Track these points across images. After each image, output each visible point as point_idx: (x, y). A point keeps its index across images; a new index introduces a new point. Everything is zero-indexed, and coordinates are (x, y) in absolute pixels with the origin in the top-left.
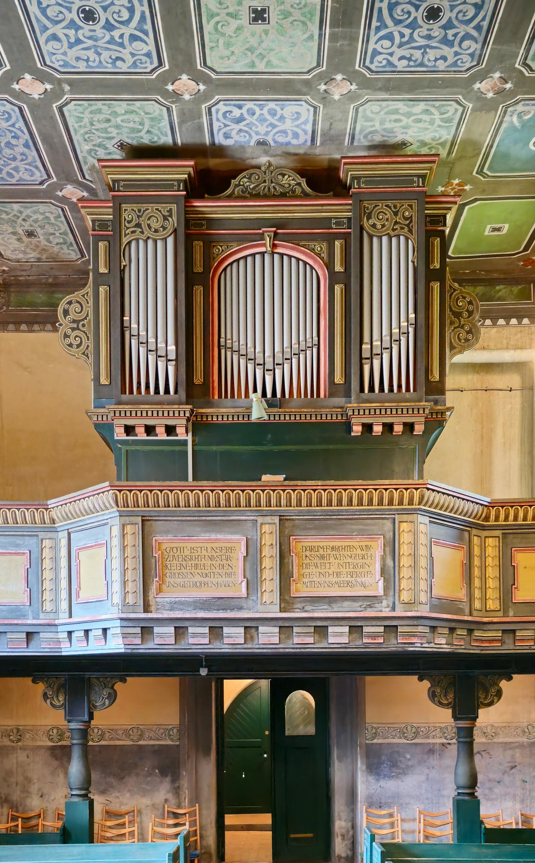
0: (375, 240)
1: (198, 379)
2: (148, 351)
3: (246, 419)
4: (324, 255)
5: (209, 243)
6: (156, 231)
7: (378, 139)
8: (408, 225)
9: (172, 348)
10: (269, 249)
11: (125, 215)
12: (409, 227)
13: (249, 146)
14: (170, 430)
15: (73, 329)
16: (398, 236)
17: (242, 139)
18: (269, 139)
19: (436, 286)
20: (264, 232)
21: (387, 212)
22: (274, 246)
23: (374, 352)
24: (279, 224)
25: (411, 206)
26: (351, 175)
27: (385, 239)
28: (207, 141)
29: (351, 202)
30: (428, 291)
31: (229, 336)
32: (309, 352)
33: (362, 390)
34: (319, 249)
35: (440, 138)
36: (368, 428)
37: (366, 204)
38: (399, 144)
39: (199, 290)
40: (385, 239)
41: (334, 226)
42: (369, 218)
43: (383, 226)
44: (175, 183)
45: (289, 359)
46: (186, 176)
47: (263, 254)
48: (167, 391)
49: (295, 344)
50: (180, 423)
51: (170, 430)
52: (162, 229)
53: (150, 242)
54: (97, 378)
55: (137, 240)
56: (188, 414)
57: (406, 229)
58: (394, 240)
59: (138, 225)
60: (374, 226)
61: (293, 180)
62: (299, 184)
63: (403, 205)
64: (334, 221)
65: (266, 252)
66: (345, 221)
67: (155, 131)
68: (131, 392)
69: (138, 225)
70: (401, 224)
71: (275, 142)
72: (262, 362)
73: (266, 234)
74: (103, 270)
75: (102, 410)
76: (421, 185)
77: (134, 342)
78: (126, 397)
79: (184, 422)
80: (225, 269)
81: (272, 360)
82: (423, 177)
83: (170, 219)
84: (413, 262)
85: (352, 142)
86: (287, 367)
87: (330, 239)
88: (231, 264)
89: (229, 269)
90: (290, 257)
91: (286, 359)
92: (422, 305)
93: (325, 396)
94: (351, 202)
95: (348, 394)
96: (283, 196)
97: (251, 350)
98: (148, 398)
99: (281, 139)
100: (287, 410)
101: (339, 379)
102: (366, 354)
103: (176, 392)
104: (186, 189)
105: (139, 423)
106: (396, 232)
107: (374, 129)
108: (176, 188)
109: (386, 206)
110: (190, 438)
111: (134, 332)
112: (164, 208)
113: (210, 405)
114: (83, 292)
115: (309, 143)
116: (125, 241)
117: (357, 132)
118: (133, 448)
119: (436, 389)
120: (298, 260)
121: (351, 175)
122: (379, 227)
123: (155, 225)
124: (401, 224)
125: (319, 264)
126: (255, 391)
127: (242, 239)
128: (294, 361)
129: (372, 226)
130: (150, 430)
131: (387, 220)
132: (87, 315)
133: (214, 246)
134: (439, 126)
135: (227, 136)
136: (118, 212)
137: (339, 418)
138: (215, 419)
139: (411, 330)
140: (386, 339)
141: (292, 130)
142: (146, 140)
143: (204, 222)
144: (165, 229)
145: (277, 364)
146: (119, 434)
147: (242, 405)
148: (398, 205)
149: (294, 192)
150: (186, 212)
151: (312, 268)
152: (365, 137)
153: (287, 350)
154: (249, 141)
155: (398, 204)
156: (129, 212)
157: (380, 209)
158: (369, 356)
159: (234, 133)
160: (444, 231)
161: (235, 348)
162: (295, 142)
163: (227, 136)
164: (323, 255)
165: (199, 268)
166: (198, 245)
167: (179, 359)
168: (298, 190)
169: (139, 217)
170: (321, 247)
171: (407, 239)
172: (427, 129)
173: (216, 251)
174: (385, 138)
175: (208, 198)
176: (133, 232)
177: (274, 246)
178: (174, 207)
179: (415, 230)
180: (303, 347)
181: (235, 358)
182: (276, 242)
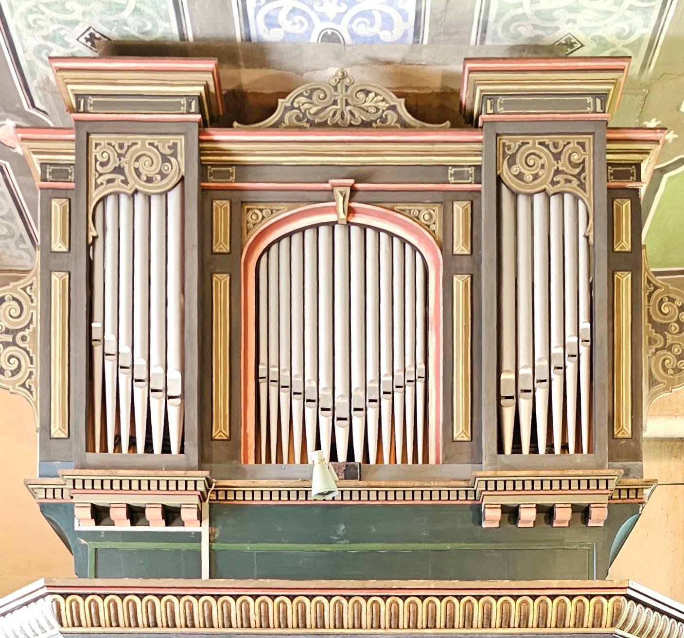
0: (522, 201)
1: (221, 431)
2: (134, 380)
3: (302, 497)
4: (437, 227)
5: (240, 204)
6: (149, 180)
7: (526, 33)
8: (577, 176)
9: (174, 375)
10: (343, 216)
11: (95, 152)
12: (579, 180)
13: (309, 43)
14: (171, 515)
15: (6, 345)
16: (561, 194)
17: (296, 30)
18: (343, 29)
19: (625, 279)
20: (334, 186)
21: (542, 155)
22: (351, 211)
23: (521, 386)
24: (361, 175)
25: (582, 145)
26: (482, 91)
27: (538, 200)
28: (239, 35)
30: (612, 285)
31: (273, 361)
32: (409, 389)
33: (501, 450)
34: (427, 217)
35: (631, 33)
36: (511, 513)
37: (505, 140)
38: (561, 44)
39: (221, 281)
40: (538, 200)
41: (452, 179)
42: (512, 162)
43: (536, 177)
44: (183, 101)
47: (332, 225)
48: (166, 449)
49: (386, 375)
50: (188, 504)
51: (171, 515)
52: (159, 177)
53: (139, 199)
54: (46, 427)
55: (117, 195)
56: (201, 487)
57: (575, 182)
58: (554, 201)
59: (119, 170)
60: (520, 176)
61: (383, 100)
62: (393, 108)
63: (569, 143)
64: (451, 171)
65: (336, 222)
66: (471, 171)
67: (149, 11)
68: (104, 449)
69: (119, 170)
70: (566, 174)
71: (353, 36)
72: (330, 406)
73: (337, 190)
74: (58, 245)
75: (54, 480)
76: (599, 109)
77: (110, 365)
78: (97, 456)
79: (196, 500)
80: (267, 250)
81: (347, 401)
82: (603, 96)
83: (173, 160)
84: (587, 238)
85: (483, 39)
86: (372, 413)
88: (278, 241)
89: (274, 248)
91: (371, 401)
92: (601, 309)
93: (437, 462)
95: (476, 458)
96: (366, 125)
97: (311, 384)
98: (132, 459)
99: (362, 30)
100: (373, 484)
101: (461, 432)
102: (507, 390)
103: (182, 451)
104: (201, 111)
105: (117, 503)
106: (557, 188)
108: (184, 109)
109: (540, 144)
110: (205, 530)
111: (110, 348)
112: (164, 142)
113: (240, 473)
114: (22, 283)
115: (410, 39)
116: (95, 195)
117: (491, 18)
118: (107, 545)
119: (628, 450)
120: (391, 235)
121: (482, 91)
122: (528, 177)
123: (147, 170)
124: (566, 174)
126: (318, 447)
127: (298, 198)
128: (386, 403)
129: (516, 176)
130: (135, 514)
131: (543, 166)
132: (31, 322)
133: (248, 210)
134: (631, 8)
135: (271, 22)
136: (85, 148)
137: (462, 496)
138: (248, 497)
139: (584, 350)
140: (542, 364)
142: (132, 28)
143: (232, 170)
144: (164, 176)
145: (356, 409)
146: (84, 522)
147: (297, 475)
148: (561, 144)
149: (384, 120)
150: (202, 152)
151: (415, 249)
152: (505, 28)
153: (372, 385)
154: (309, 33)
155: (561, 140)
156: (103, 147)
158: (513, 394)
159: (282, 17)
160: (636, 190)
162: (386, 36)
163: (271, 22)
164: (433, 227)
165: (222, 245)
166: (221, 208)
167: (187, 394)
168: (392, 118)
169: (120, 156)
170: (431, 213)
171: (576, 199)
172: (609, 13)
173: (251, 218)
174: (539, 32)
175: (237, 127)
176: (110, 181)
177: (351, 211)
178: (181, 141)
179: (589, 185)
181: (285, 395)
182: (354, 205)
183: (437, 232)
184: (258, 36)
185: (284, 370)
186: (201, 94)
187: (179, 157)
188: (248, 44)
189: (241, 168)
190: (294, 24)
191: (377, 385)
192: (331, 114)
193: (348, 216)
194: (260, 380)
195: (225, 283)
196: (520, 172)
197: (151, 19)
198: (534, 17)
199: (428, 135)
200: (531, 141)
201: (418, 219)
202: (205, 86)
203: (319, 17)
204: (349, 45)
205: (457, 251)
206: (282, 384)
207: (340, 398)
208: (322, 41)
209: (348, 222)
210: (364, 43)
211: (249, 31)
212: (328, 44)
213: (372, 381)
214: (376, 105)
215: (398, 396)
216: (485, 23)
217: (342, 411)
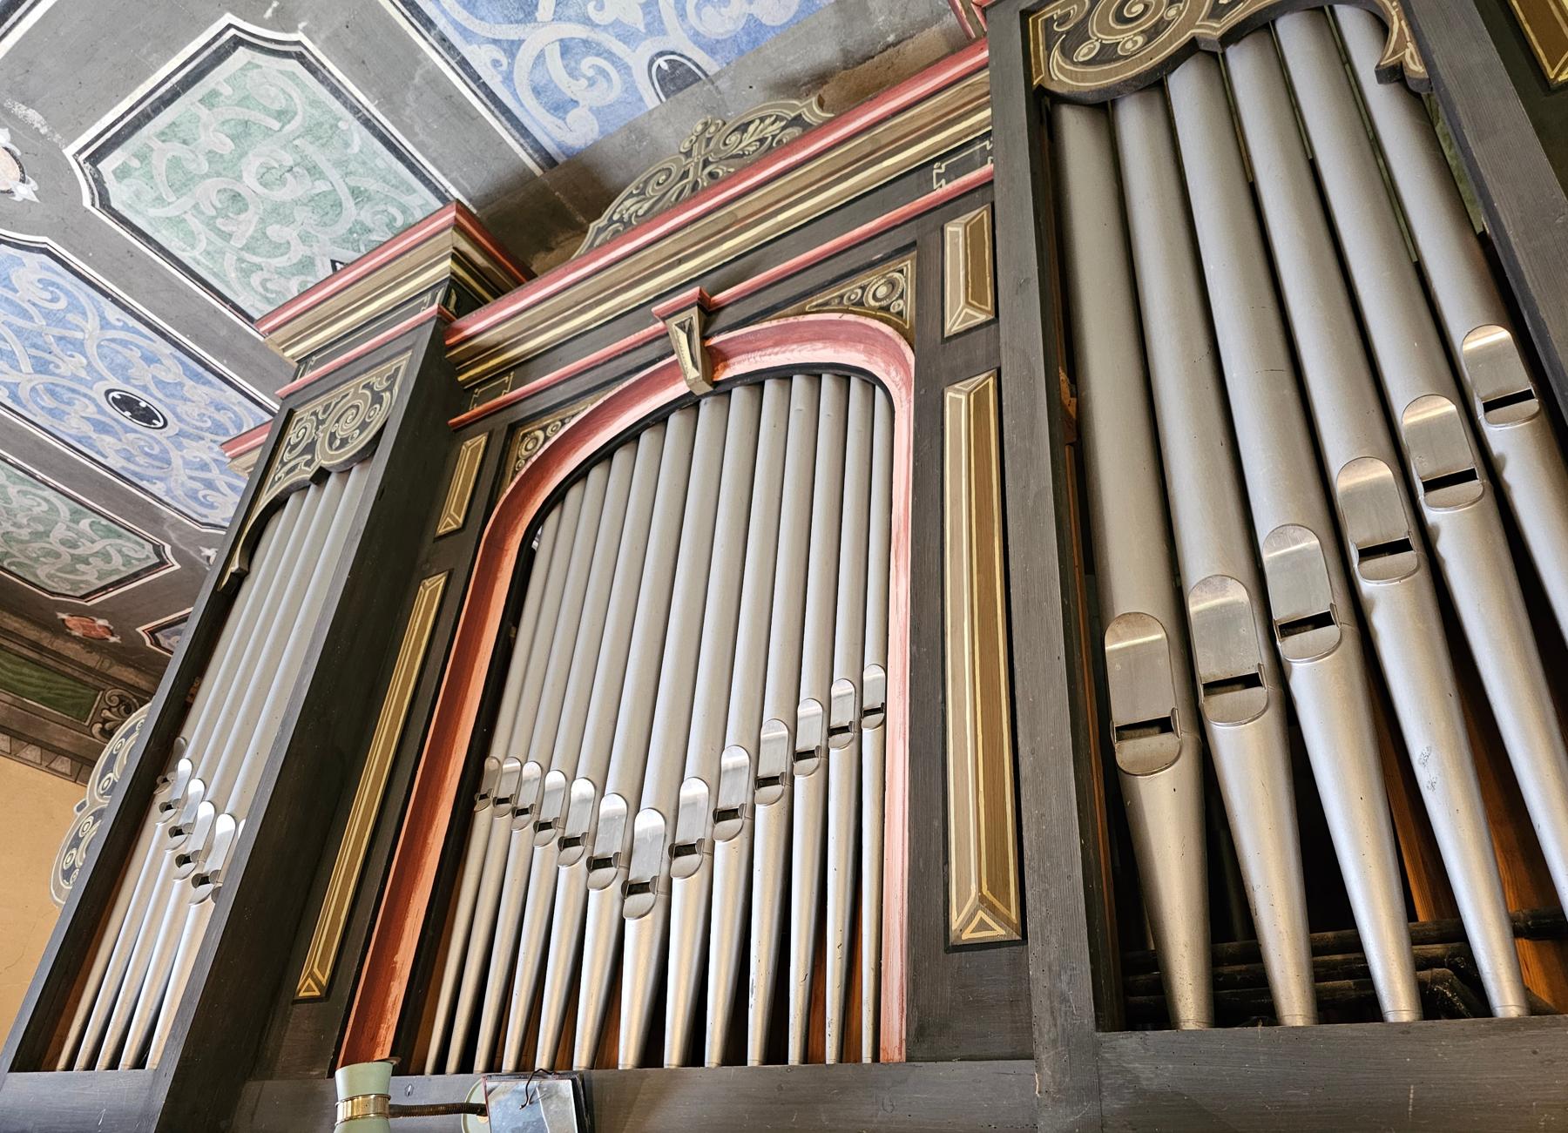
13: (651, 113)
17: (613, 91)
29: (986, 54)
84: (1393, 74)
94: (986, 54)
154: (630, 87)
184: (559, 146)
188: (556, 172)
199: (854, 120)
208: (667, 97)
210: (741, 53)
212: (680, 95)
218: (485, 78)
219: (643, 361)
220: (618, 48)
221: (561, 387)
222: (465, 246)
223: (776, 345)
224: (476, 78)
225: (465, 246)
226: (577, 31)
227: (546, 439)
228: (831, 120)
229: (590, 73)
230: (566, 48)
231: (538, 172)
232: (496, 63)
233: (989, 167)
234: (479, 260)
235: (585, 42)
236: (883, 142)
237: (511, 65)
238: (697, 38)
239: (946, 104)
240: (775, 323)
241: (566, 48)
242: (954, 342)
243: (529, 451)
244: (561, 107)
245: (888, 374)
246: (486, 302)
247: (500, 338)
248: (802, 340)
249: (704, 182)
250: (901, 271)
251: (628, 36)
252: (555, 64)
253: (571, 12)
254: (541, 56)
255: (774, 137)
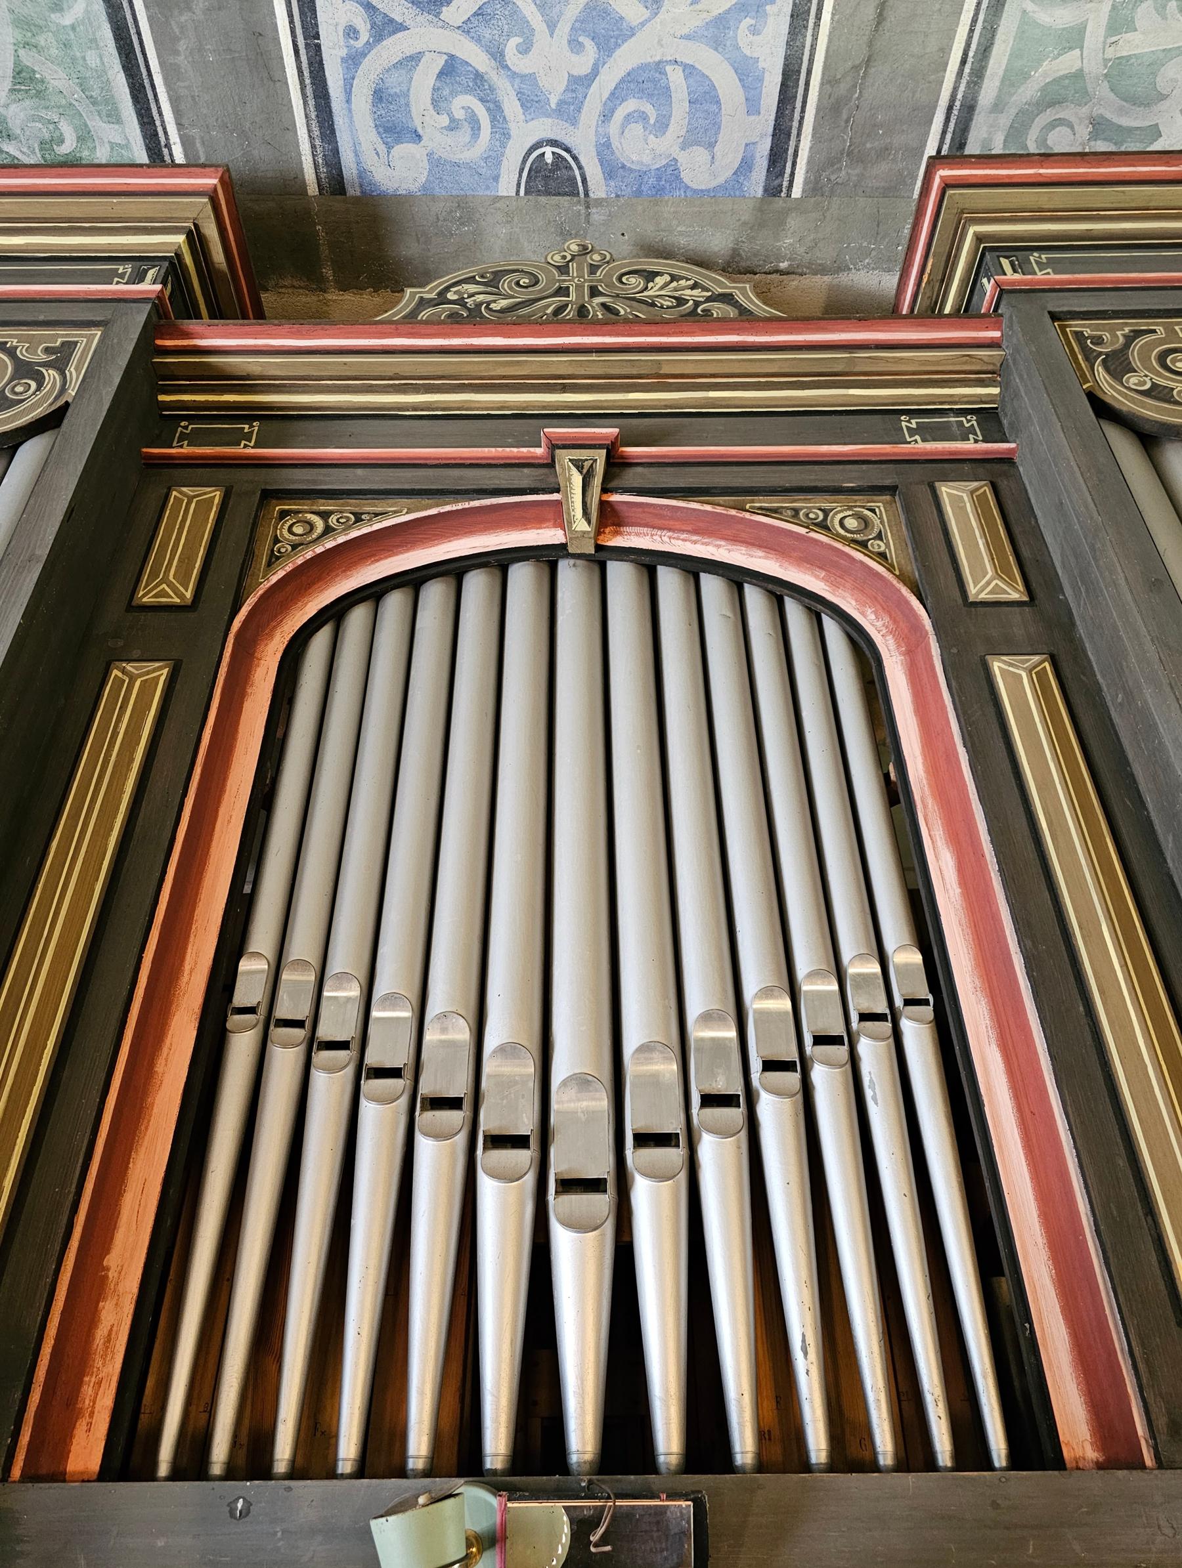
5: (258, 497)
10: (581, 525)
13: (499, 198)
18: (583, 141)
26: (979, 238)
31: (303, 944)
32: (872, 1053)
34: (851, 523)
39: (137, 687)
42: (1118, 365)
45: (727, 1101)
46: (181, 239)
47: (548, 558)
61: (693, 287)
71: (612, 170)
72: (527, 1124)
73: (565, 457)
80: (336, 613)
81: (602, 1102)
83: (51, 375)
86: (718, 1158)
87: (909, 486)
88: (374, 593)
89: (358, 617)
90: (692, 568)
91: (709, 1100)
97: (448, 1032)
99: (640, 149)
107: (1069, 62)
121: (979, 238)
125: (866, 584)
135: (395, 130)
141: (689, 70)
145: (643, 1140)
153: (712, 1034)
154: (494, 159)
157: (1162, 341)
161: (337, 1023)
164: (878, 546)
177: (608, 517)
180: (823, 1017)
181: (329, 1090)
182: (615, 498)
183: (892, 554)
184: (362, 173)
185: (343, 976)
186: (180, 247)
187: (71, 370)
188: (336, 203)
189: (276, 425)
190: (454, 125)
191: (732, 1034)
192: (549, 311)
193: (599, 532)
194: (234, 1020)
195: (147, 688)
196: (1154, 384)
197: (68, 110)
198: (1104, 90)
200: (1158, 328)
201: (827, 528)
202: (189, 235)
203: (520, 94)
204: (599, 202)
205: (978, 590)
206: (326, 1031)
207: (572, 1092)
208: (526, 193)
209: (599, 548)
210: (638, 193)
211: (336, 152)
212: (543, 199)
213: (707, 1018)
214: (676, 294)
215: (826, 1080)
216: (969, 108)
217: (581, 1149)
218: (325, 41)
219: (505, 485)
220: (511, 107)
221: (359, 471)
222: (211, 231)
223: (695, 532)
224: (312, 34)
225: (211, 231)
226: (479, 60)
227: (328, 530)
228: (779, 319)
229: (459, 114)
230: (451, 68)
231: (313, 189)
232: (351, 32)
233: (1013, 445)
234: (218, 256)
235: (479, 77)
236: (858, 369)
237: (369, 46)
238: (604, 149)
239: (938, 363)
240: (708, 508)
241: (451, 68)
242: (981, 610)
243: (301, 535)
244: (395, 130)
245: (863, 614)
246: (245, 317)
247: (257, 370)
248: (735, 540)
249: (570, 313)
250: (873, 511)
251: (531, 102)
252: (424, 80)
253: (487, 33)
254: (414, 59)
255: (697, 304)
